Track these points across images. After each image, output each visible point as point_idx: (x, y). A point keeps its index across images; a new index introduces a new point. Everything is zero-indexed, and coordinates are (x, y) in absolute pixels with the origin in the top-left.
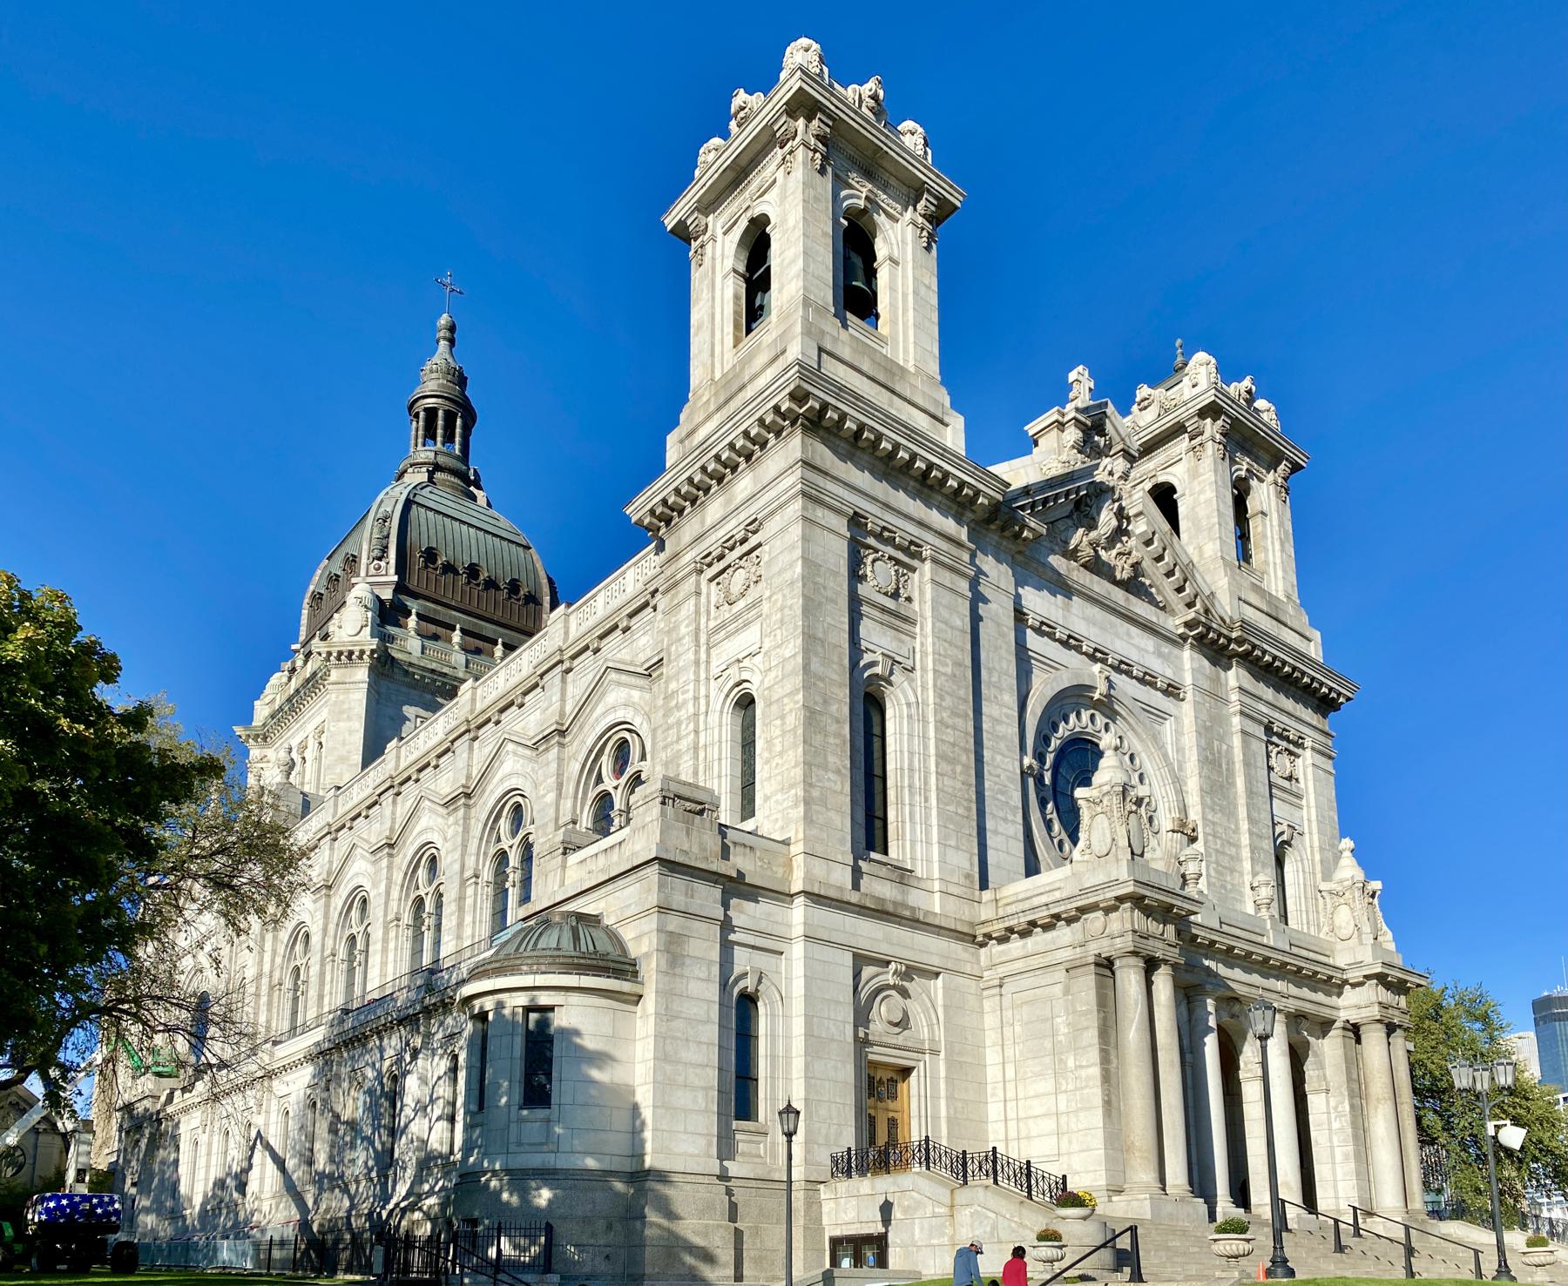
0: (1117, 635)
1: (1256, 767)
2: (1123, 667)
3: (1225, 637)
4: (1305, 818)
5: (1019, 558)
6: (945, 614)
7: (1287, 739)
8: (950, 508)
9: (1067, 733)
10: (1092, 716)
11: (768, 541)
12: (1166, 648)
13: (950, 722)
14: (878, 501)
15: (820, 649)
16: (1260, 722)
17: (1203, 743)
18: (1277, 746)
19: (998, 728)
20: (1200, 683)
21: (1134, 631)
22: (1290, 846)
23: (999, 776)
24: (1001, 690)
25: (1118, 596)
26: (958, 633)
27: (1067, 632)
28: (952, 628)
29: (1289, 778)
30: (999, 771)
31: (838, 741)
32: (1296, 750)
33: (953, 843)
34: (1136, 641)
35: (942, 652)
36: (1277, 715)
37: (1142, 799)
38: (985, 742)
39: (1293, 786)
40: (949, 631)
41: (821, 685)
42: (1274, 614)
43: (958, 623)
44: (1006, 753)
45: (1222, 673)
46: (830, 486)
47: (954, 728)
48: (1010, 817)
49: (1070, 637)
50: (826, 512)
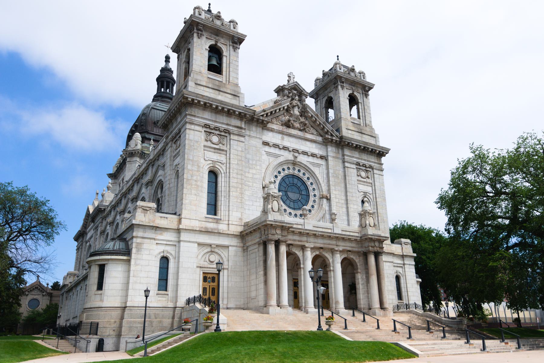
7: (366, 167)
11: (181, 134)
13: (236, 177)
15: (191, 163)
16: (353, 164)
23: (255, 189)
26: (240, 152)
27: (282, 146)
28: (237, 151)
30: (255, 188)
31: (196, 186)
32: (368, 169)
33: (235, 210)
35: (234, 158)
36: (360, 161)
40: (236, 151)
41: (191, 172)
43: (240, 149)
44: (257, 182)
47: (237, 178)
48: (258, 200)
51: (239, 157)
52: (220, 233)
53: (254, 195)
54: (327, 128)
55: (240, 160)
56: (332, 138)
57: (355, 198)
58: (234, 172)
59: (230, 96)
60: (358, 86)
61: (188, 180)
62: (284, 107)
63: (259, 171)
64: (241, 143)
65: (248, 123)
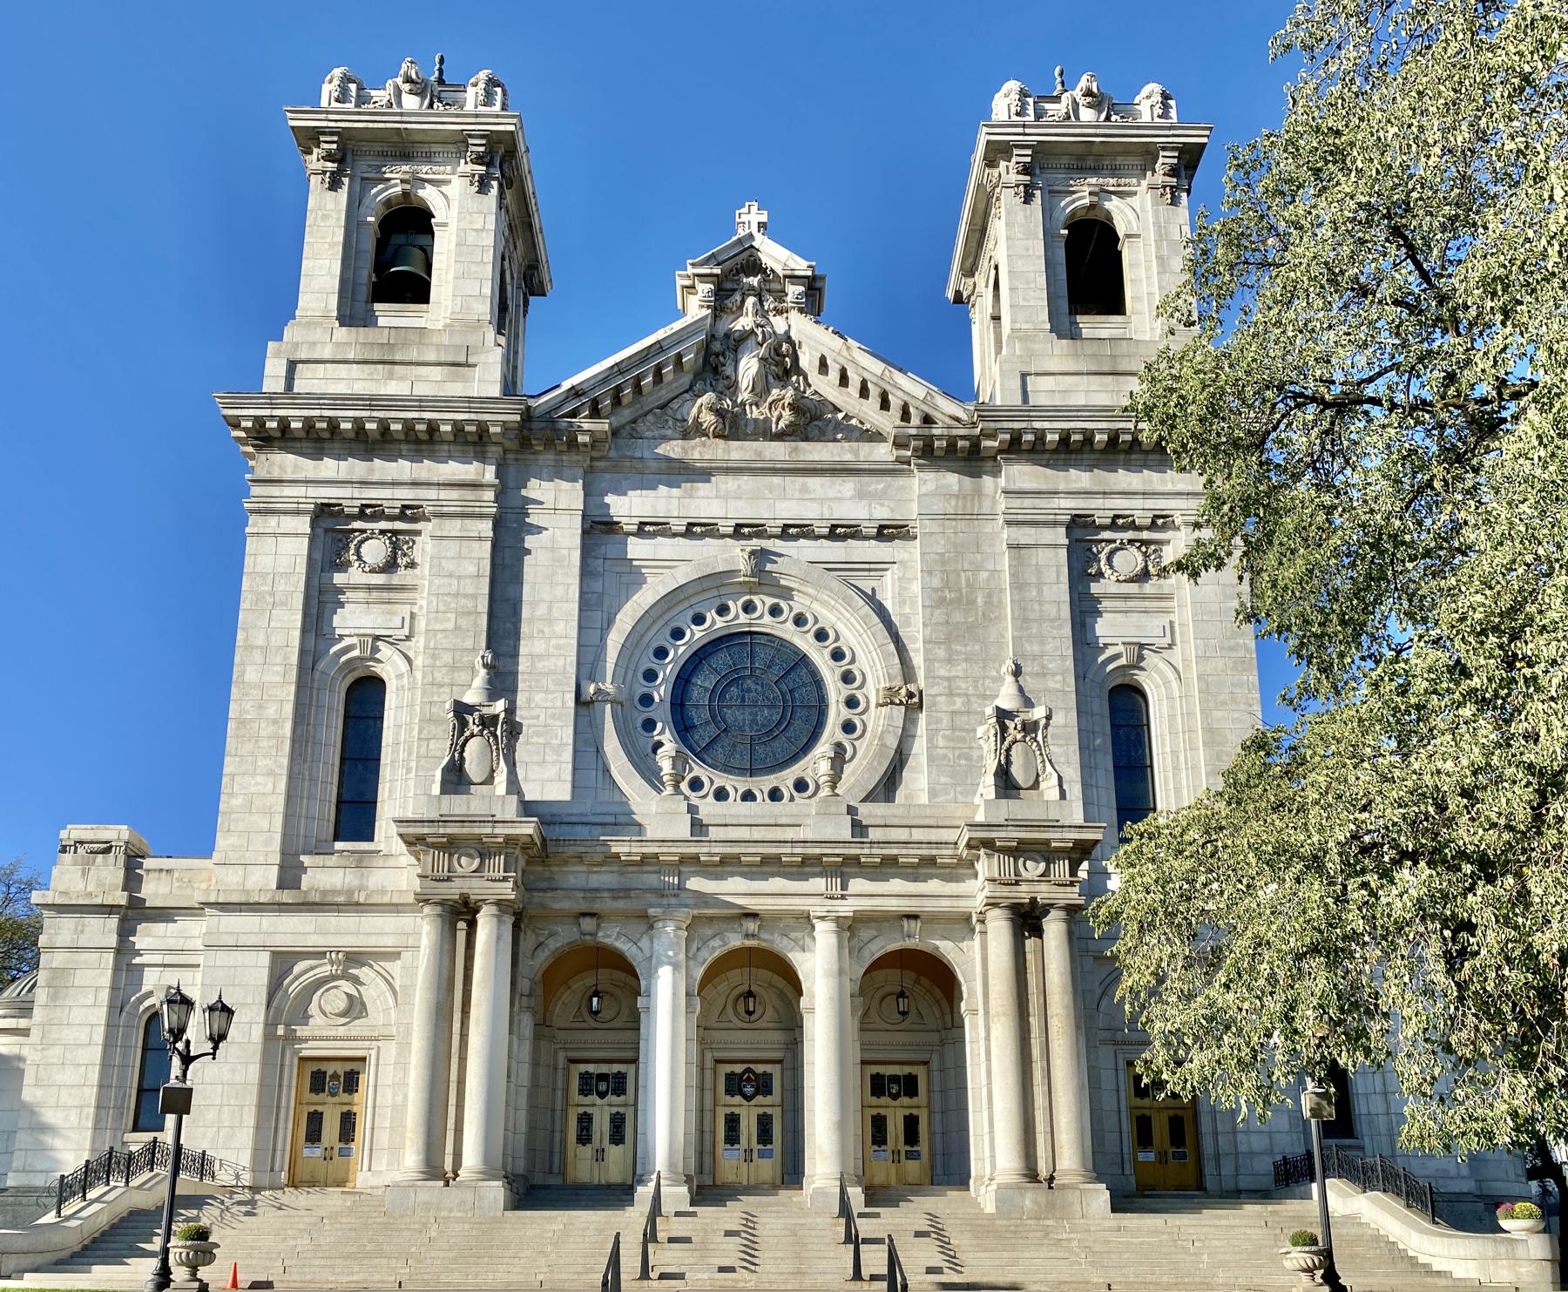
0: (785, 498)
1: (1039, 585)
2: (792, 531)
3: (963, 437)
4: (1176, 625)
5: (602, 464)
6: (449, 566)
7: (1133, 526)
8: (463, 452)
9: (698, 635)
10: (748, 608)
12: (877, 484)
14: (352, 483)
16: (1055, 524)
17: (936, 582)
18: (1115, 541)
19: (539, 665)
20: (935, 509)
21: (814, 483)
22: (1142, 669)
24: (550, 621)
25: (778, 451)
26: (468, 581)
28: (459, 577)
29: (1144, 575)
34: (820, 493)
35: (441, 608)
36: (1098, 502)
37: (498, 716)
38: (520, 685)
39: (1149, 587)
42: (1106, 369)
43: (472, 569)
44: (551, 687)
45: (987, 480)
46: (288, 491)
49: (691, 525)
50: (283, 517)
51: (463, 601)
52: (358, 904)
53: (535, 740)
54: (900, 394)
55: (469, 613)
56: (926, 432)
57: (1059, 678)
58: (438, 663)
59: (436, 373)
60: (1119, 161)
61: (242, 723)
62: (679, 357)
63: (562, 641)
64: (476, 545)
65: (516, 460)
